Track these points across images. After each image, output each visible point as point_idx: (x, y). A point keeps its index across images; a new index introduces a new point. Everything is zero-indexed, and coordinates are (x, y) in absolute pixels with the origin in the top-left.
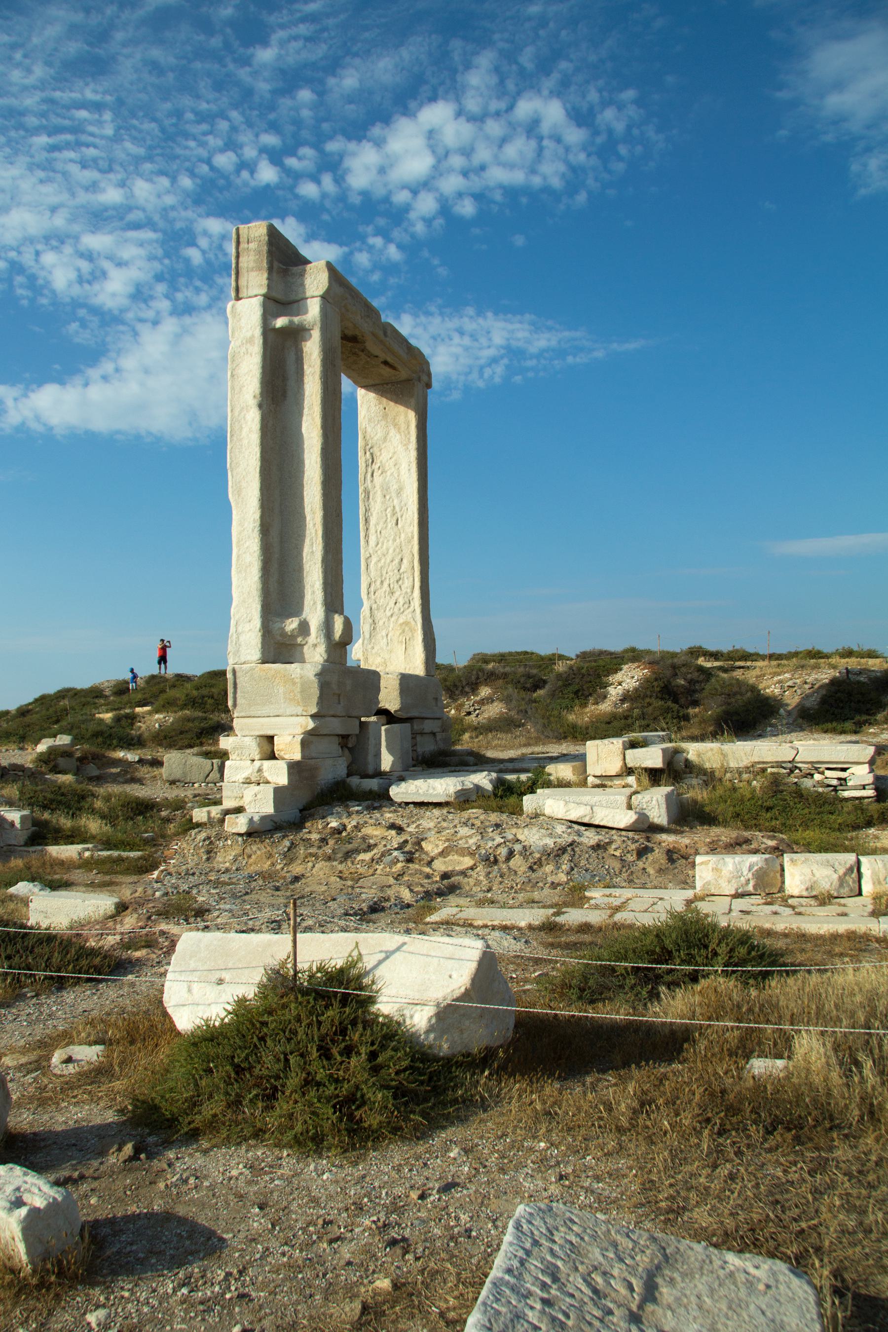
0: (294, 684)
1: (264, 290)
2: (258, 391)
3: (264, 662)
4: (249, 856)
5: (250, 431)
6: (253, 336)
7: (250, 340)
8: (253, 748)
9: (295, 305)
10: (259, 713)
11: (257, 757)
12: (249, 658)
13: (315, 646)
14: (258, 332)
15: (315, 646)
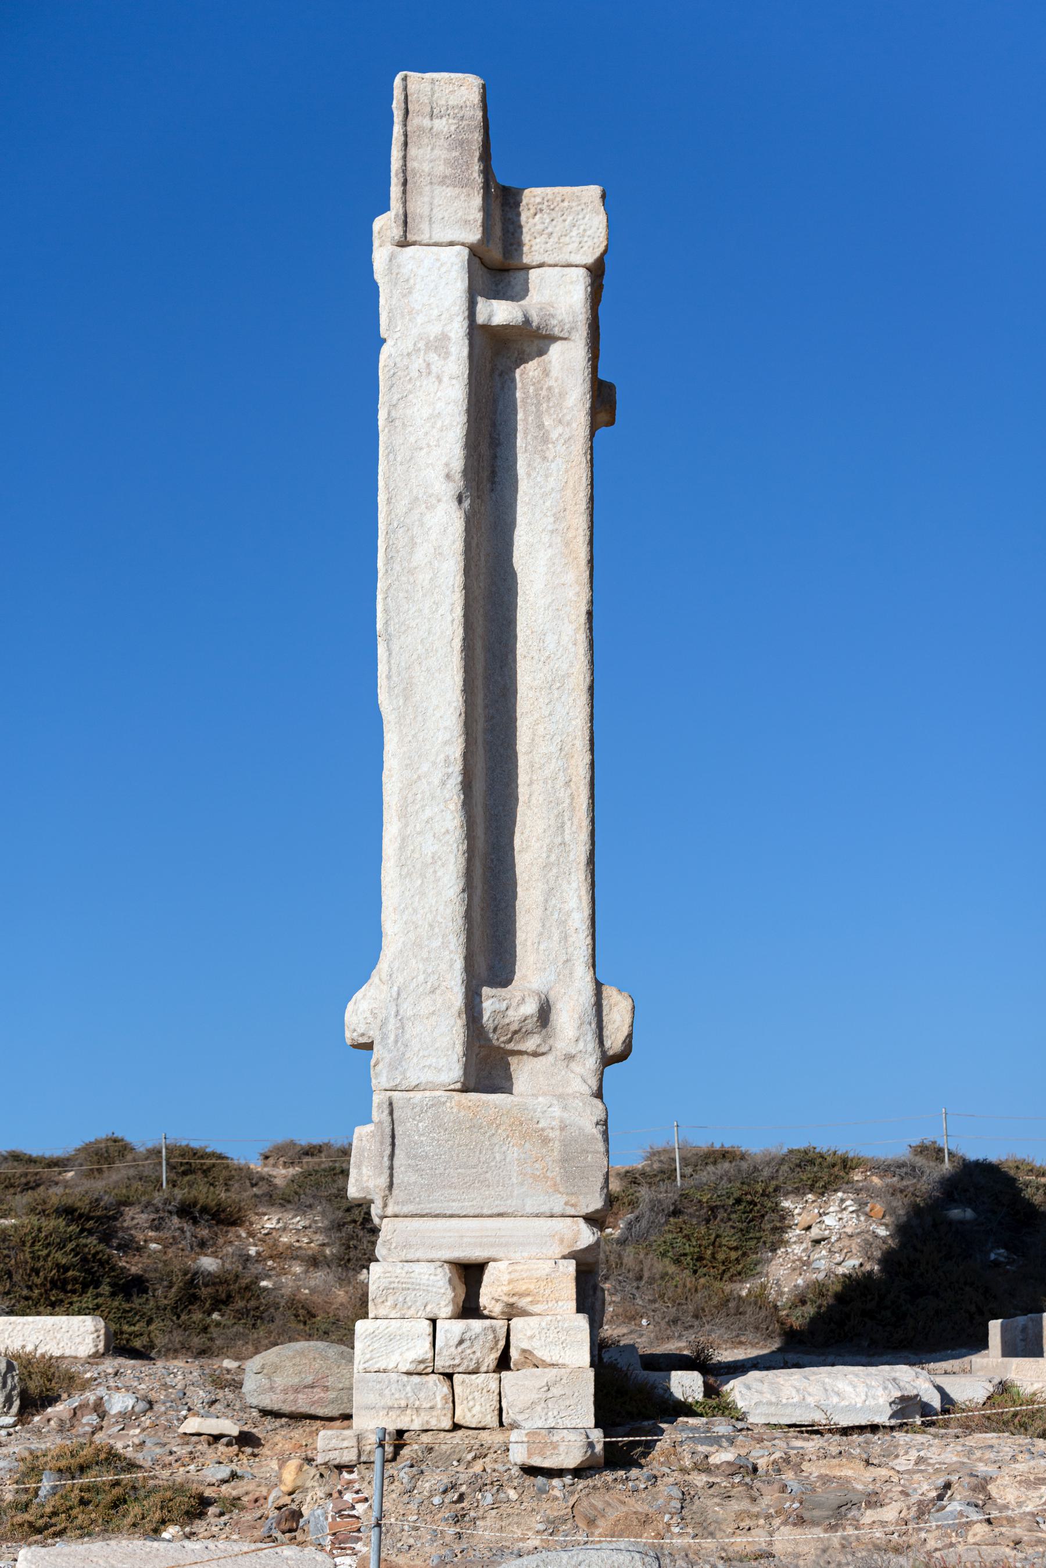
0: (546, 1141)
1: (474, 235)
2: (458, 464)
3: (465, 1090)
4: (591, 1522)
5: (438, 552)
6: (444, 337)
7: (439, 344)
8: (441, 1292)
9: (522, 273)
10: (454, 1207)
11: (446, 1310)
12: (427, 1077)
13: (570, 1058)
14: (458, 329)
15: (570, 1058)
